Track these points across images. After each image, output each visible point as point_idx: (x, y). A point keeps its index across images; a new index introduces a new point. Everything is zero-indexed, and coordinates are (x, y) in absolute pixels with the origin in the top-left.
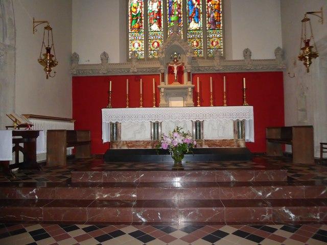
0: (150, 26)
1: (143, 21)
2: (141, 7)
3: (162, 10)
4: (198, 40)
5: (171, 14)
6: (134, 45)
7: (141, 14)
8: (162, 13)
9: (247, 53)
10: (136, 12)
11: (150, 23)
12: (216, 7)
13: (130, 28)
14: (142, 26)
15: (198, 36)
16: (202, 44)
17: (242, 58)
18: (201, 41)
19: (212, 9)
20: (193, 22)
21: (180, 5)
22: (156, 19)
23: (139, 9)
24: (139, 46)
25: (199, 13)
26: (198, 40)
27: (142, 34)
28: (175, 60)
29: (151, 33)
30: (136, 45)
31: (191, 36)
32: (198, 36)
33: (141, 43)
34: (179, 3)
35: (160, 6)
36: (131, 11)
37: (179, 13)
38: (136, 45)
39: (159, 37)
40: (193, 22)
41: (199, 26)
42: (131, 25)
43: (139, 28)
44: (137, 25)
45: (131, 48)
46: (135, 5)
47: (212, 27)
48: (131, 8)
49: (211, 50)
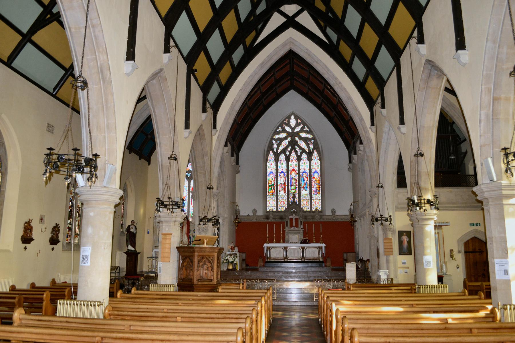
5: (291, 186)
9: (333, 211)
16: (309, 203)
17: (331, 214)
23: (273, 182)
27: (275, 197)
29: (279, 196)
37: (296, 185)
43: (273, 193)
45: (268, 204)
47: (315, 193)
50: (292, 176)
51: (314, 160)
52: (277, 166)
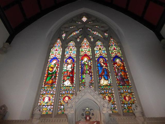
0: (63, 82)
1: (57, 78)
2: (57, 68)
3: (75, 70)
4: (110, 95)
6: (44, 100)
7: (56, 72)
8: (75, 72)
10: (52, 71)
11: (64, 80)
12: (121, 68)
13: (44, 83)
14: (55, 82)
15: (110, 91)
18: (113, 96)
19: (118, 69)
20: (103, 79)
21: (91, 66)
22: (70, 76)
23: (55, 69)
24: (50, 100)
25: (108, 72)
26: (110, 95)
28: (88, 118)
29: (63, 88)
30: (47, 100)
31: (103, 91)
32: (110, 91)
33: (51, 98)
34: (90, 65)
35: (74, 67)
36: (48, 70)
38: (47, 100)
39: (71, 92)
40: (103, 79)
41: (109, 83)
42: (46, 81)
43: (52, 83)
44: (51, 81)
46: (52, 66)
48: (49, 67)
49: (125, 105)
50: (83, 62)
51: (112, 45)
52: (63, 52)
